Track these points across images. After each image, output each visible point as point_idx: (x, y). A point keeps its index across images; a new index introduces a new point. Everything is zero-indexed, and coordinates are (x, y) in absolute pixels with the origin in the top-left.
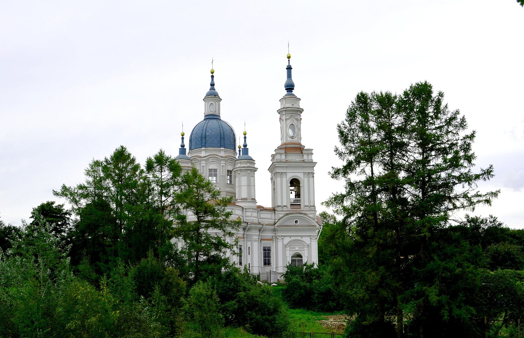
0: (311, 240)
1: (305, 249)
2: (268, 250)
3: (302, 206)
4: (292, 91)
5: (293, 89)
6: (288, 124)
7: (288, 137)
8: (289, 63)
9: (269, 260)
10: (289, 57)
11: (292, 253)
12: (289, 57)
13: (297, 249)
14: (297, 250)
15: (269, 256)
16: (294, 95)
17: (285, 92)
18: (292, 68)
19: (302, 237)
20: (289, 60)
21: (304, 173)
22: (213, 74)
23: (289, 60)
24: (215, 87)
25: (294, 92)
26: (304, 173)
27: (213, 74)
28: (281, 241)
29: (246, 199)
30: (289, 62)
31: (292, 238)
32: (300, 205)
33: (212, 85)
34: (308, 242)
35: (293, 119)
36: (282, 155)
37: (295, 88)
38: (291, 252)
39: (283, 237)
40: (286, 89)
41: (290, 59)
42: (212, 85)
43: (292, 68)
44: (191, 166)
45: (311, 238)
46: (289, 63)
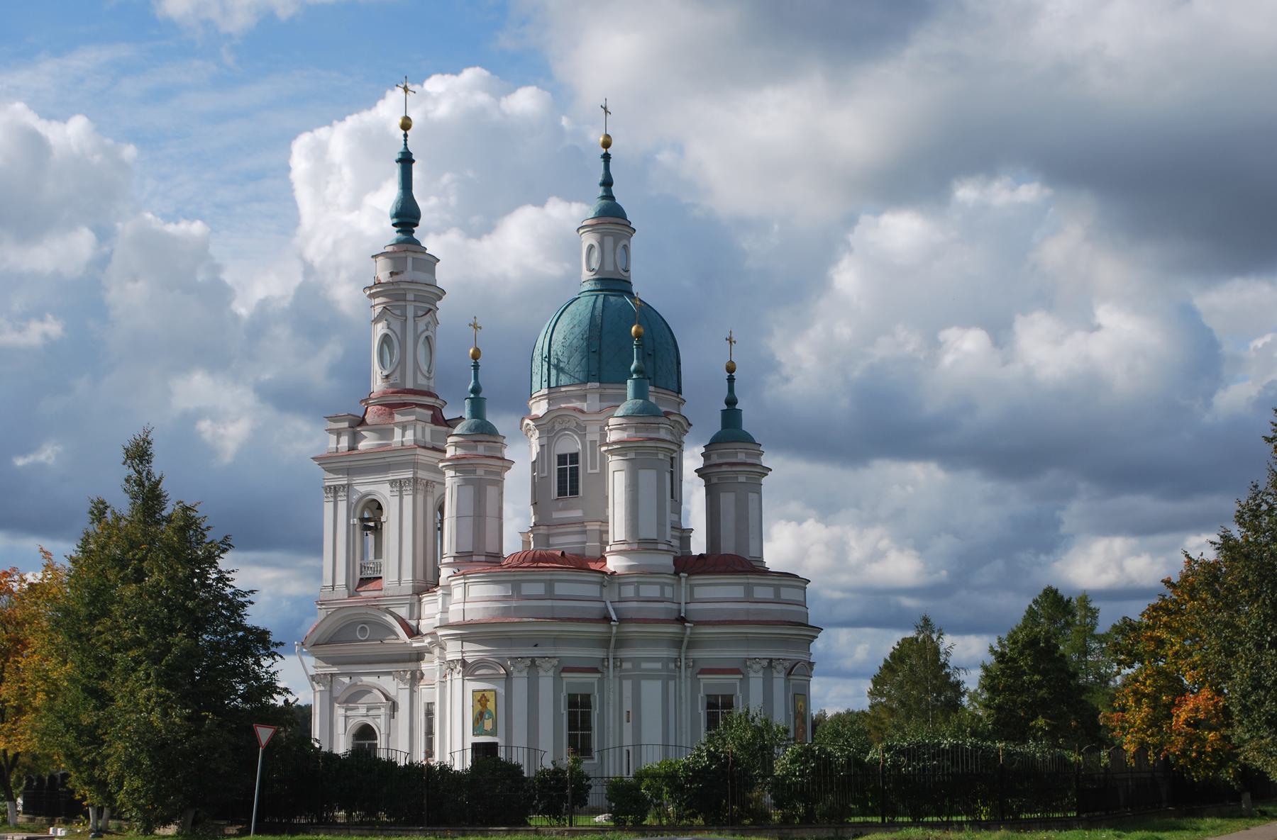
1: (383, 710)
2: (723, 707)
3: (385, 583)
4: (413, 232)
5: (417, 225)
8: (406, 144)
9: (586, 739)
11: (354, 723)
14: (360, 715)
15: (587, 725)
16: (417, 243)
17: (393, 234)
18: (413, 161)
19: (378, 674)
20: (406, 136)
21: (392, 482)
22: (609, 151)
23: (406, 136)
24: (615, 190)
25: (418, 233)
26: (392, 482)
27: (609, 151)
29: (654, 542)
30: (406, 140)
32: (381, 578)
33: (607, 183)
34: (392, 693)
37: (421, 222)
40: (394, 225)
41: (408, 132)
42: (607, 183)
43: (413, 161)
44: (669, 437)
46: (406, 144)
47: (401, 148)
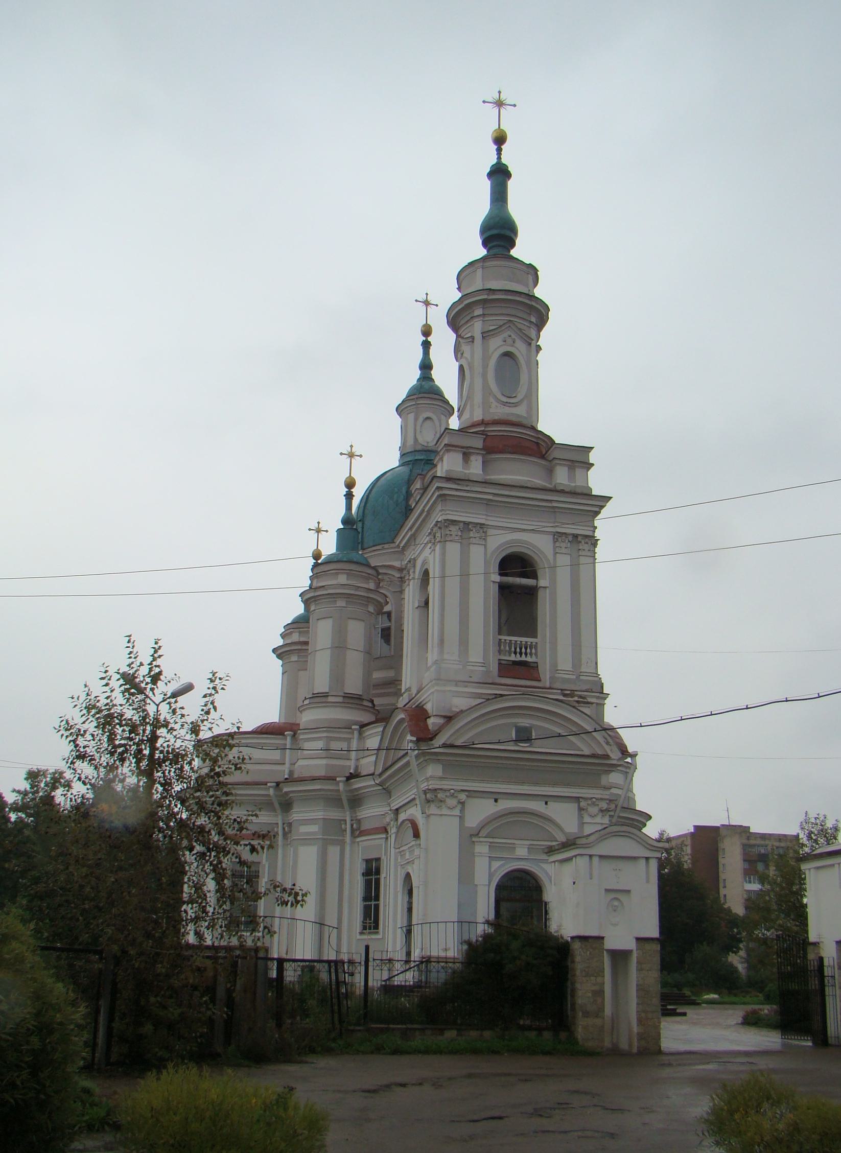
0: (581, 817)
6: (491, 350)
7: (492, 400)
8: (499, 158)
10: (500, 140)
11: (501, 869)
12: (500, 140)
13: (522, 852)
21: (558, 536)
28: (457, 812)
31: (506, 804)
35: (513, 336)
36: (473, 458)
38: (496, 864)
39: (463, 797)
45: (581, 809)
47: (494, 161)
